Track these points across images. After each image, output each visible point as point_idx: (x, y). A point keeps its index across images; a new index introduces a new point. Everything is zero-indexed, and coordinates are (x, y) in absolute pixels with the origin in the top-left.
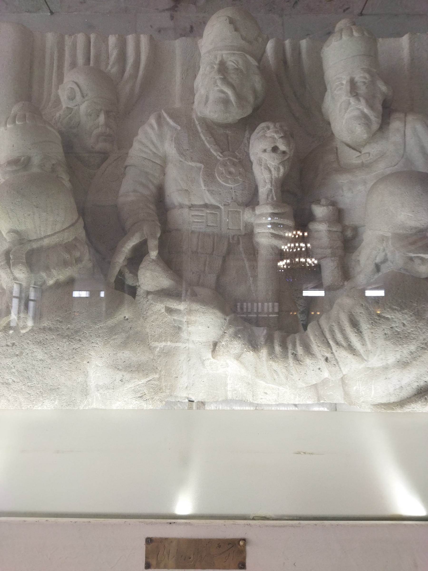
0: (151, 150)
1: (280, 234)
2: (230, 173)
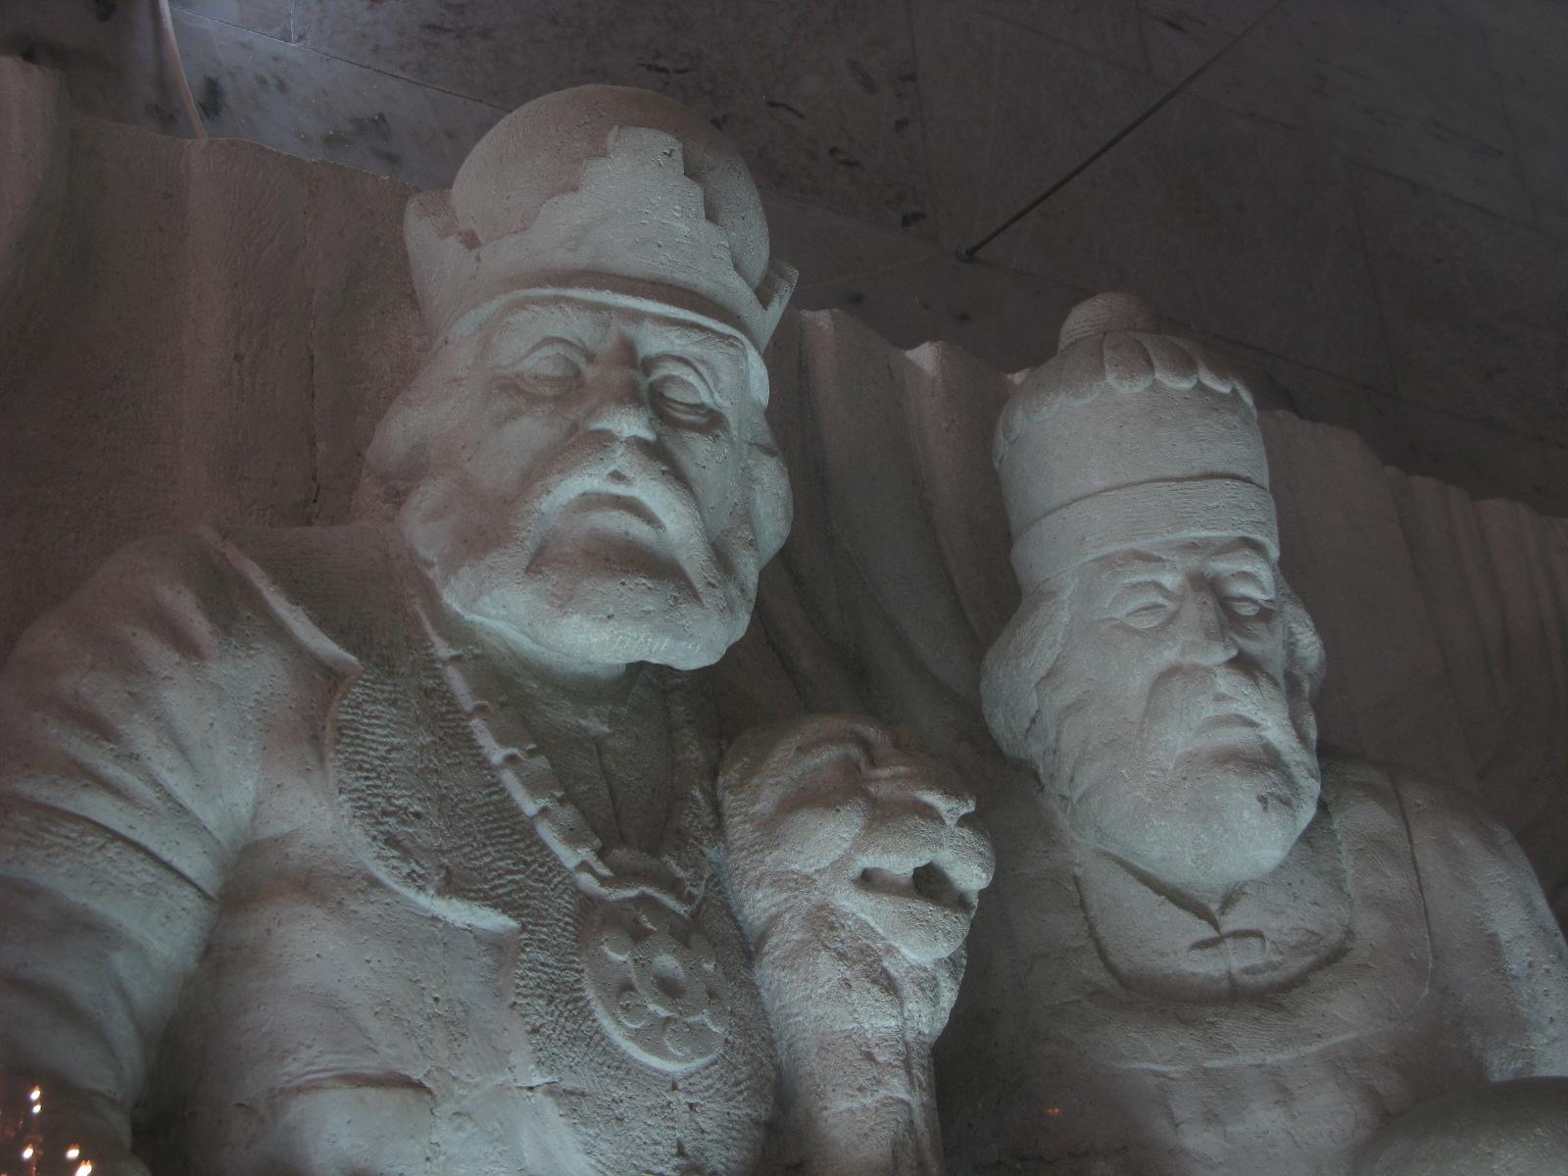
0: (156, 784)
2: (668, 988)
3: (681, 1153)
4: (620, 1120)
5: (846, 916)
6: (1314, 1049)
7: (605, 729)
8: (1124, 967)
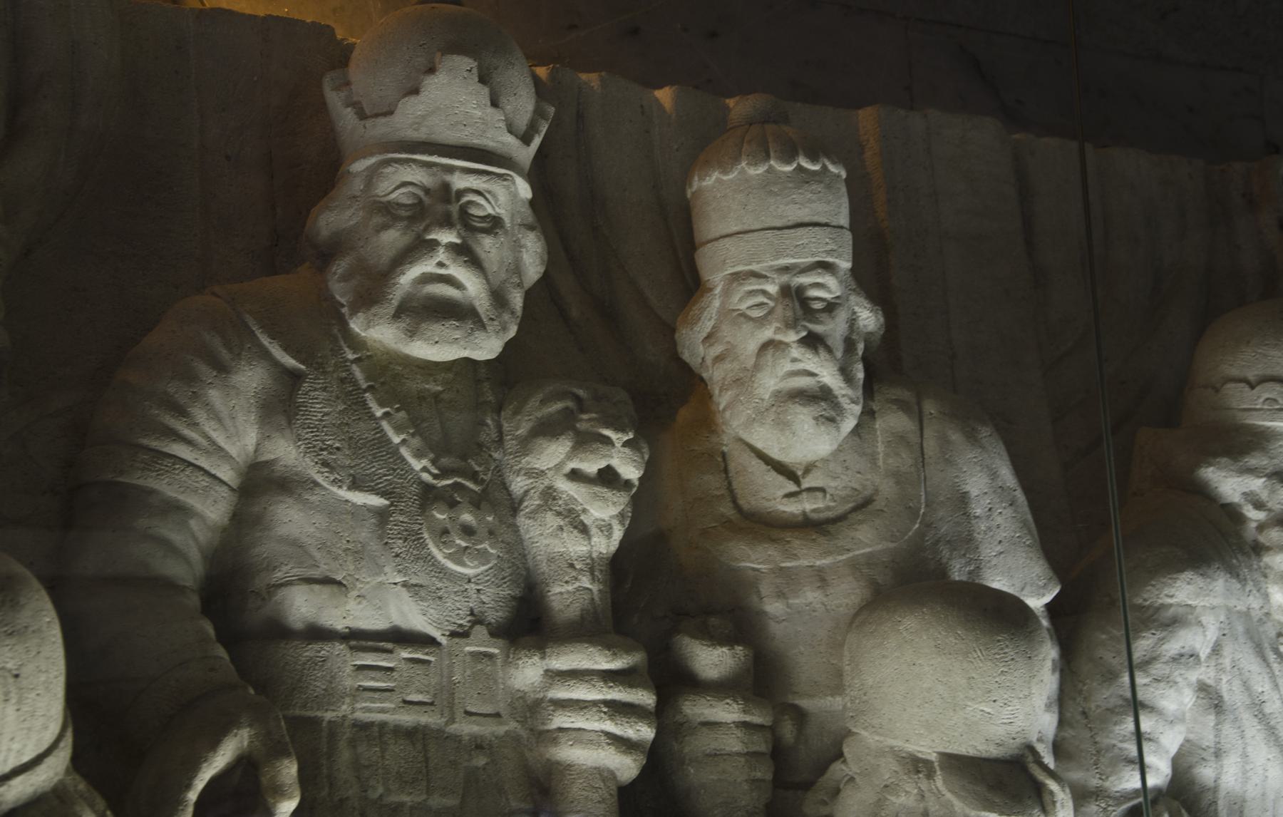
0: (208, 438)
1: (625, 735)
2: (468, 531)
3: (472, 614)
4: (440, 598)
5: (562, 492)
6: (844, 557)
7: (440, 388)
8: (746, 507)
